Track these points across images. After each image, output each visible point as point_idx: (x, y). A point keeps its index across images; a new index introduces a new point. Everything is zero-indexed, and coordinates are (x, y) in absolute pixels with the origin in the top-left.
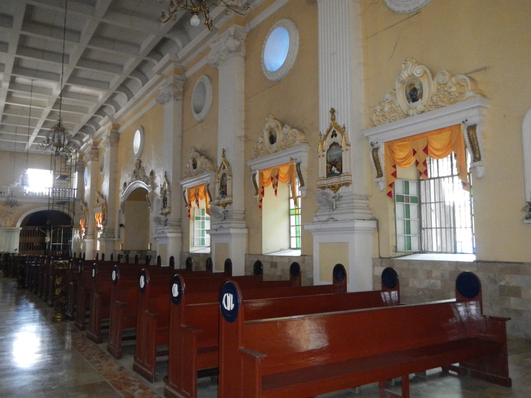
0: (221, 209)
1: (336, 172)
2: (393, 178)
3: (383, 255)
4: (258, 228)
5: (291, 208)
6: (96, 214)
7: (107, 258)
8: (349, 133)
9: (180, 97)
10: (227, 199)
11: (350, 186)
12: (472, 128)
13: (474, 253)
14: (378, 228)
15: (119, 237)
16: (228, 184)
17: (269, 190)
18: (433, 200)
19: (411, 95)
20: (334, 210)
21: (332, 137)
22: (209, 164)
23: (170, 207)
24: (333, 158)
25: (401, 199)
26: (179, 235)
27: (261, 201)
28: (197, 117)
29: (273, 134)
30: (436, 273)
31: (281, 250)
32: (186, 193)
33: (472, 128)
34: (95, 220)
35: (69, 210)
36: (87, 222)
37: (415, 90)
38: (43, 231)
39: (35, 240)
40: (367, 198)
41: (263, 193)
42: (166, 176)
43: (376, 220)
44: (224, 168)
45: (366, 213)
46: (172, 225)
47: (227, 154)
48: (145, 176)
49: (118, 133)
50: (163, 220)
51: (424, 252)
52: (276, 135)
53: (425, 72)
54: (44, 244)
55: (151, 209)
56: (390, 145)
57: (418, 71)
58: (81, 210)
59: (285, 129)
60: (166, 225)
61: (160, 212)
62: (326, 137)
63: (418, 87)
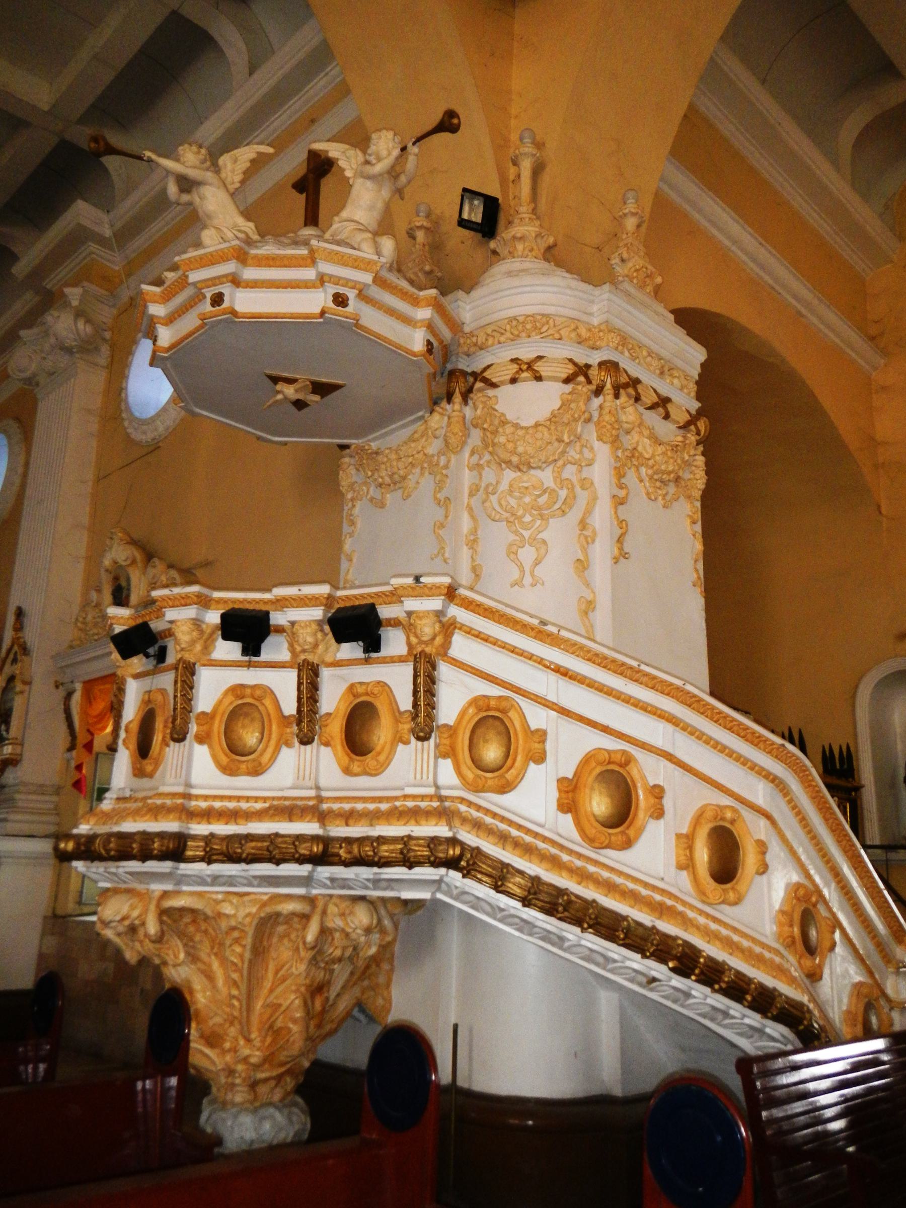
3: (60, 912)
21: (12, 664)
45: (39, 822)
63: (124, 584)
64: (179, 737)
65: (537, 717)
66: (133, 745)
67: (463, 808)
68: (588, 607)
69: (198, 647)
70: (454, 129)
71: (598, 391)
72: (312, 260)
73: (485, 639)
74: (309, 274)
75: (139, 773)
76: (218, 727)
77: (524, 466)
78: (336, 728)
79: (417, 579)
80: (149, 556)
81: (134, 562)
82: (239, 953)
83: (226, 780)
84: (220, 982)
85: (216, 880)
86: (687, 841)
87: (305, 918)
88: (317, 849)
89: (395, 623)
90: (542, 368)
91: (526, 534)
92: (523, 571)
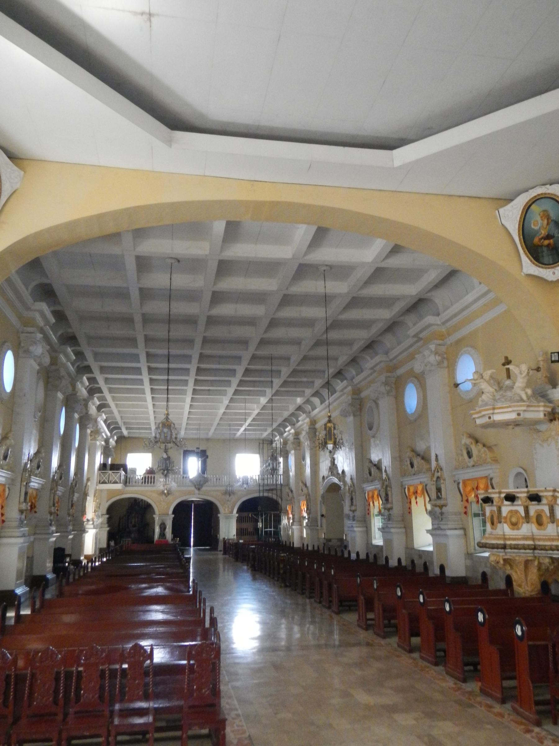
0: (386, 513)
2: (466, 503)
7: (310, 548)
9: (358, 413)
12: (491, 479)
14: (465, 534)
15: (321, 526)
16: (389, 493)
20: (440, 521)
21: (437, 472)
23: (356, 506)
26: (365, 529)
29: (412, 461)
32: (366, 495)
34: (301, 508)
35: (277, 495)
36: (294, 509)
38: (255, 517)
39: (248, 526)
42: (351, 479)
46: (358, 521)
48: (338, 474)
50: (351, 516)
54: (257, 529)
55: (344, 504)
56: (464, 482)
58: (287, 496)
63: (470, 450)
64: (500, 522)
66: (490, 522)
69: (500, 502)
72: (510, 407)
74: (510, 409)
75: (492, 528)
76: (508, 520)
78: (534, 520)
79: (546, 488)
80: (477, 441)
81: (472, 443)
82: (522, 567)
83: (512, 531)
84: (519, 573)
85: (514, 553)
87: (534, 560)
88: (533, 547)
89: (543, 496)
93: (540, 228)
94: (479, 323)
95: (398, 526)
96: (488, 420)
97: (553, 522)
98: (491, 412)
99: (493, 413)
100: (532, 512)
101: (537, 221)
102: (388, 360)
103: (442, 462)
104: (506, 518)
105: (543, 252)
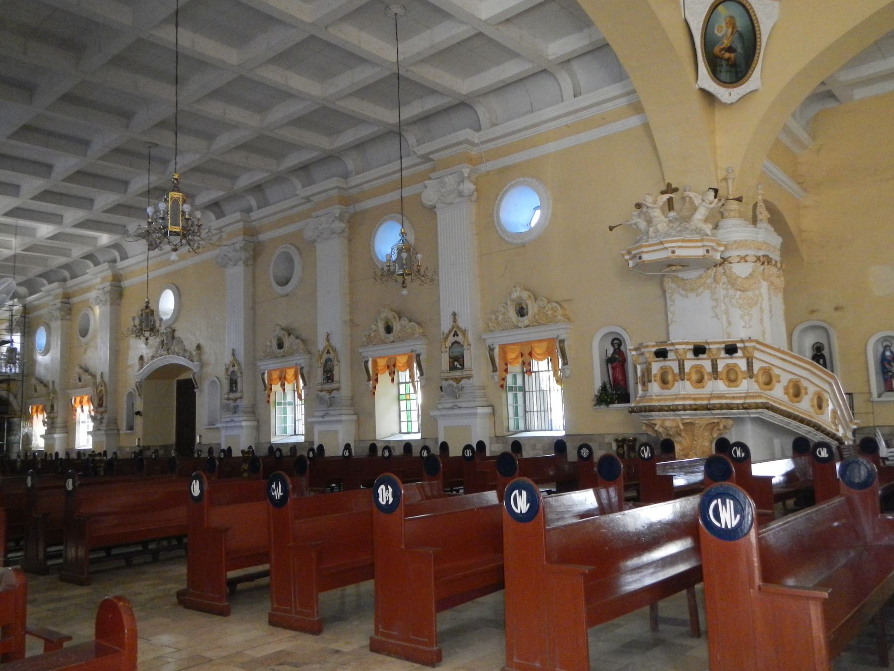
1: (458, 366)
2: (504, 373)
3: (498, 435)
4: (371, 415)
5: (401, 393)
6: (73, 398)
8: (471, 337)
9: (250, 262)
10: (334, 385)
11: (471, 379)
12: (562, 342)
13: (564, 430)
14: (494, 413)
17: (384, 378)
18: (534, 389)
19: (520, 312)
20: (457, 398)
21: (454, 336)
22: (301, 346)
23: (242, 391)
24: (456, 354)
25: (511, 389)
26: (255, 423)
27: (375, 388)
28: (279, 290)
29: (390, 324)
30: (539, 446)
31: (392, 435)
33: (562, 342)
37: (522, 308)
40: (484, 388)
41: (377, 380)
42: (233, 355)
43: (492, 406)
44: (328, 352)
46: (245, 413)
47: (331, 337)
48: (185, 350)
49: (120, 287)
51: (529, 431)
52: (393, 326)
53: (530, 296)
56: (503, 348)
57: (525, 295)
59: (403, 322)
60: (235, 412)
61: (226, 396)
62: (448, 335)
63: (525, 307)
65: (776, 371)
67: (762, 394)
68: (764, 333)
70: (741, 201)
71: (763, 264)
72: (702, 240)
73: (763, 351)
74: (700, 244)
77: (744, 290)
78: (724, 376)
83: (696, 390)
86: (812, 400)
90: (748, 259)
91: (746, 312)
92: (746, 323)
93: (723, 35)
94: (552, 147)
95: (347, 412)
96: (670, 254)
97: (751, 377)
98: (679, 244)
99: (680, 247)
100: (721, 366)
101: (722, 27)
102: (345, 186)
103: (464, 322)
104: (689, 374)
105: (722, 65)
